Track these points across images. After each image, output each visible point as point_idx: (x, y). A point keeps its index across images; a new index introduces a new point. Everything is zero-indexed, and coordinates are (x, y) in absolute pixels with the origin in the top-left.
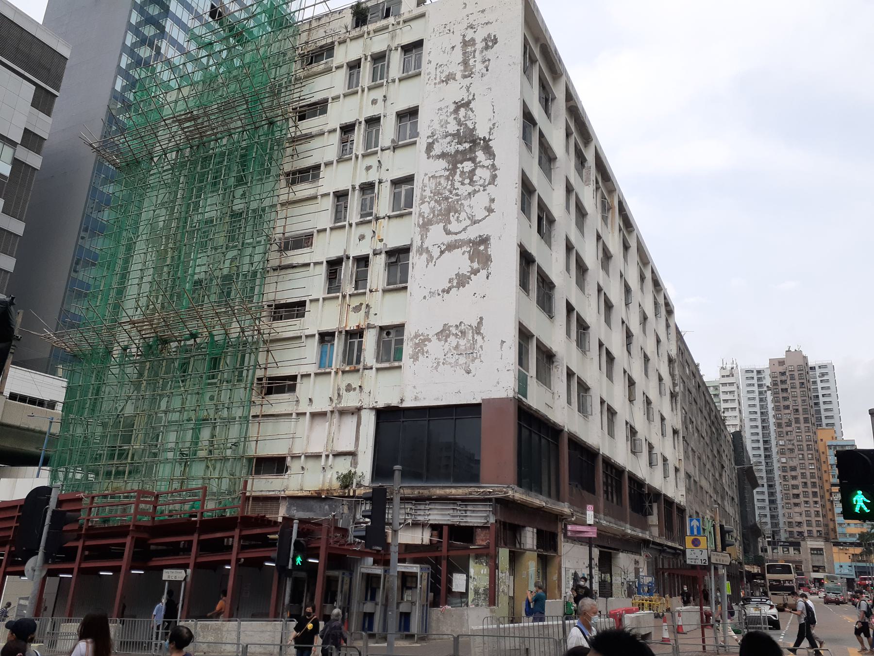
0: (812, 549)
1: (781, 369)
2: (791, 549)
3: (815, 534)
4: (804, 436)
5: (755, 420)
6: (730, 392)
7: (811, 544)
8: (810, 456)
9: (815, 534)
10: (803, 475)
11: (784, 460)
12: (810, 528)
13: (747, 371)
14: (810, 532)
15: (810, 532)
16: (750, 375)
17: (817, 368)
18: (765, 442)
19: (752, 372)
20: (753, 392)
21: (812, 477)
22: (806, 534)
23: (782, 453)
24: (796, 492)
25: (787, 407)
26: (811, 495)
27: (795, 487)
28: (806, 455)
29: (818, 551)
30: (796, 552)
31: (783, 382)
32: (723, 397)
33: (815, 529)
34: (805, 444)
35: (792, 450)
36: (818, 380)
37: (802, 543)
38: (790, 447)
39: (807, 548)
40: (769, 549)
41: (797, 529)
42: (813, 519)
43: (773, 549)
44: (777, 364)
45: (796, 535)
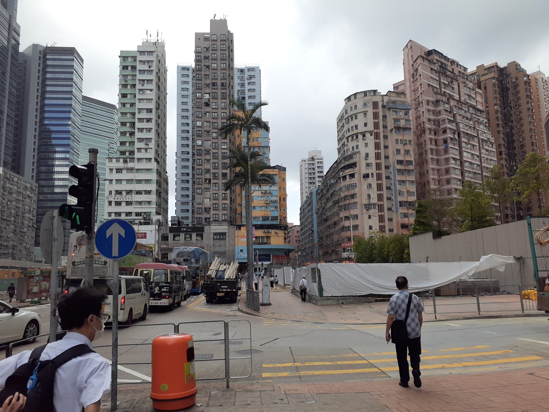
0: (215, 234)
1: (207, 44)
2: (194, 235)
3: (221, 219)
4: (219, 113)
5: (187, 117)
6: (148, 62)
10: (215, 158)
13: (184, 68)
16: (186, 72)
17: (246, 71)
19: (188, 69)
21: (224, 158)
24: (208, 176)
26: (220, 177)
27: (208, 171)
29: (221, 236)
30: (199, 238)
31: (206, 58)
32: (139, 67)
36: (246, 82)
37: (206, 228)
40: (171, 236)
42: (221, 202)
43: (174, 237)
44: (202, 39)
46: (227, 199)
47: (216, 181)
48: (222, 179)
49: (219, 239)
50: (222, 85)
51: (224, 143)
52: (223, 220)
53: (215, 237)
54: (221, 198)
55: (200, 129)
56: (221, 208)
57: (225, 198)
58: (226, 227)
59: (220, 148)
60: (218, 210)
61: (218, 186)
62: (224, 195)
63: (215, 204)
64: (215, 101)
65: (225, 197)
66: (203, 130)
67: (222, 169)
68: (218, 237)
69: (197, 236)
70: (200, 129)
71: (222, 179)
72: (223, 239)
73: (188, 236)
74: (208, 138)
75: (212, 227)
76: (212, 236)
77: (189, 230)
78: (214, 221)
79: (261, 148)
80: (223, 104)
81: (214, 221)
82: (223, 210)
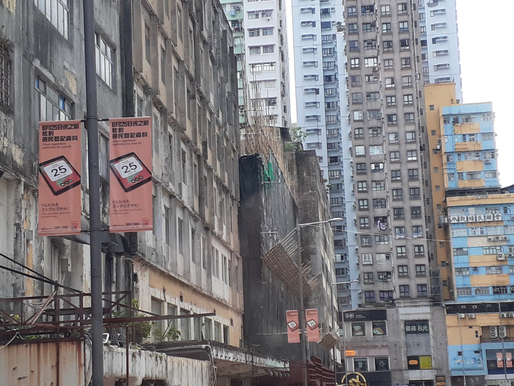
0: (407, 323)
2: (369, 326)
3: (414, 292)
4: (399, 96)
7: (407, 312)
8: (409, 136)
9: (414, 292)
11: (360, 150)
12: (405, 281)
14: (405, 288)
15: (405, 288)
18: (328, 79)
20: (313, 37)
21: (412, 178)
22: (396, 295)
23: (356, 137)
25: (371, 44)
26: (408, 214)
28: (401, 135)
29: (418, 326)
30: (378, 331)
33: (413, 283)
34: (400, 111)
35: (376, 130)
37: (390, 312)
38: (374, 123)
39: (397, 322)
41: (381, 286)
45: (378, 300)
46: (423, 256)
47: (400, 223)
48: (412, 218)
49: (414, 332)
50: (403, 43)
51: (412, 151)
52: (419, 297)
53: (408, 329)
54: (411, 255)
55: (360, 125)
56: (413, 272)
57: (419, 255)
58: (428, 309)
59: (404, 161)
60: (408, 277)
61: (406, 233)
62: (417, 250)
63: (402, 266)
64: (391, 74)
65: (419, 251)
66: (365, 126)
67: (411, 199)
68: (414, 328)
69: (374, 327)
70: (360, 125)
71: (412, 218)
72: (421, 332)
73: (357, 328)
74: (376, 140)
75: (401, 311)
76: (402, 326)
77: (360, 316)
78: (401, 298)
79: (480, 153)
80: (405, 80)
81: (401, 298)
82: (417, 276)
